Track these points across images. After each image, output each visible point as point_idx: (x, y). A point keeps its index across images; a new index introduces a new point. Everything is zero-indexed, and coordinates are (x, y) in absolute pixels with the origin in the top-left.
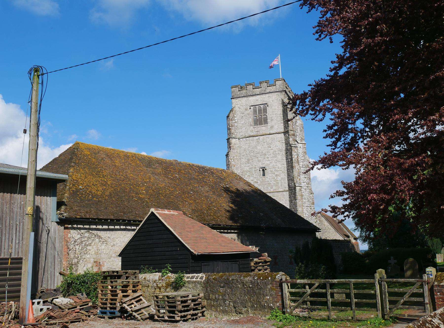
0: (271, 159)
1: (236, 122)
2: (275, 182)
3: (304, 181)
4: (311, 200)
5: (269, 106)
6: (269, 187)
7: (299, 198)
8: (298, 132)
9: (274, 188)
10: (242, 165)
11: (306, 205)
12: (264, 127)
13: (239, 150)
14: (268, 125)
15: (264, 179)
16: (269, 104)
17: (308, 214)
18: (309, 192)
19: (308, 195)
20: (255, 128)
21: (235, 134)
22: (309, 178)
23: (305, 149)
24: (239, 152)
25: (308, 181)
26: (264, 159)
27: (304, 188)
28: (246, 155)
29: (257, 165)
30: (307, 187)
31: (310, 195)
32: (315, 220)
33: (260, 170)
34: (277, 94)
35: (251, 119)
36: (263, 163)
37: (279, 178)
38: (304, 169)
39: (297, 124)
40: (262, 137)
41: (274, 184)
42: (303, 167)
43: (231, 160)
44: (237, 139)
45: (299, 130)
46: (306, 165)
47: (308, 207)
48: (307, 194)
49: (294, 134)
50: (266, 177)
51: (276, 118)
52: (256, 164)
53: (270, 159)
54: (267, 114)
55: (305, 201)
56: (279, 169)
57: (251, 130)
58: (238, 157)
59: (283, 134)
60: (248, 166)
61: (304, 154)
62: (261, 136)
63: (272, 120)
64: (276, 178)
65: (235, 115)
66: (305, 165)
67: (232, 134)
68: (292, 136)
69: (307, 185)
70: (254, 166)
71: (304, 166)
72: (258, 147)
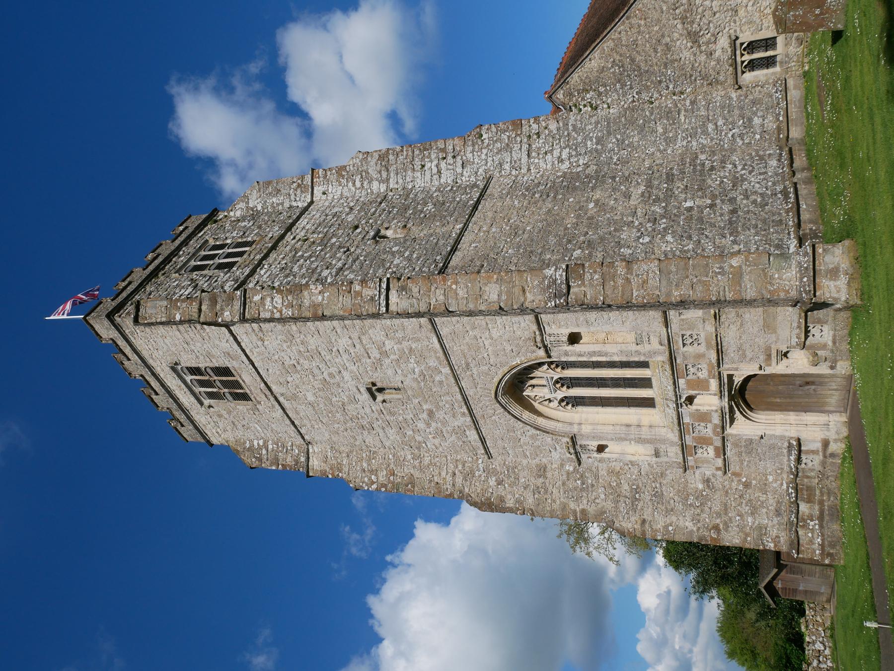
0: (333, 366)
1: (265, 442)
2: (412, 361)
3: (435, 170)
4: (504, 137)
5: (176, 359)
6: (437, 378)
7: (442, 297)
8: (282, 204)
9: (432, 363)
10: (387, 444)
12: (244, 378)
13: (342, 448)
14: (229, 366)
15: (410, 393)
16: (171, 359)
17: (562, 149)
18: (473, 145)
19: (485, 151)
20: (258, 399)
21: (297, 451)
22: (425, 149)
23: (329, 173)
24: (349, 447)
25: (433, 156)
26: (338, 385)
27: (459, 170)
28: (349, 431)
29: (368, 405)
30: (454, 157)
31: (487, 141)
32: (584, 110)
33: (384, 401)
34: (132, 339)
35: (238, 407)
36: (355, 390)
37: (389, 345)
38: (392, 175)
39: (259, 208)
40: (274, 388)
41: (417, 363)
42: (388, 180)
43: (373, 483)
44: (311, 450)
45: (274, 200)
46: (378, 168)
47: (534, 146)
48: (483, 157)
49: (210, 299)
50: (400, 385)
51: (199, 345)
52: (368, 410)
53: (332, 370)
54: (200, 366)
55: (507, 166)
56: (358, 346)
57: (269, 409)
58: (364, 455)
59: (232, 328)
60: (381, 431)
61: (343, 177)
62: (273, 390)
63: (209, 355)
64: (392, 357)
65: (248, 445)
66: (380, 172)
67: (297, 462)
68: (218, 307)
69: (450, 160)
70: (376, 415)
71: (384, 174)
72: (311, 398)
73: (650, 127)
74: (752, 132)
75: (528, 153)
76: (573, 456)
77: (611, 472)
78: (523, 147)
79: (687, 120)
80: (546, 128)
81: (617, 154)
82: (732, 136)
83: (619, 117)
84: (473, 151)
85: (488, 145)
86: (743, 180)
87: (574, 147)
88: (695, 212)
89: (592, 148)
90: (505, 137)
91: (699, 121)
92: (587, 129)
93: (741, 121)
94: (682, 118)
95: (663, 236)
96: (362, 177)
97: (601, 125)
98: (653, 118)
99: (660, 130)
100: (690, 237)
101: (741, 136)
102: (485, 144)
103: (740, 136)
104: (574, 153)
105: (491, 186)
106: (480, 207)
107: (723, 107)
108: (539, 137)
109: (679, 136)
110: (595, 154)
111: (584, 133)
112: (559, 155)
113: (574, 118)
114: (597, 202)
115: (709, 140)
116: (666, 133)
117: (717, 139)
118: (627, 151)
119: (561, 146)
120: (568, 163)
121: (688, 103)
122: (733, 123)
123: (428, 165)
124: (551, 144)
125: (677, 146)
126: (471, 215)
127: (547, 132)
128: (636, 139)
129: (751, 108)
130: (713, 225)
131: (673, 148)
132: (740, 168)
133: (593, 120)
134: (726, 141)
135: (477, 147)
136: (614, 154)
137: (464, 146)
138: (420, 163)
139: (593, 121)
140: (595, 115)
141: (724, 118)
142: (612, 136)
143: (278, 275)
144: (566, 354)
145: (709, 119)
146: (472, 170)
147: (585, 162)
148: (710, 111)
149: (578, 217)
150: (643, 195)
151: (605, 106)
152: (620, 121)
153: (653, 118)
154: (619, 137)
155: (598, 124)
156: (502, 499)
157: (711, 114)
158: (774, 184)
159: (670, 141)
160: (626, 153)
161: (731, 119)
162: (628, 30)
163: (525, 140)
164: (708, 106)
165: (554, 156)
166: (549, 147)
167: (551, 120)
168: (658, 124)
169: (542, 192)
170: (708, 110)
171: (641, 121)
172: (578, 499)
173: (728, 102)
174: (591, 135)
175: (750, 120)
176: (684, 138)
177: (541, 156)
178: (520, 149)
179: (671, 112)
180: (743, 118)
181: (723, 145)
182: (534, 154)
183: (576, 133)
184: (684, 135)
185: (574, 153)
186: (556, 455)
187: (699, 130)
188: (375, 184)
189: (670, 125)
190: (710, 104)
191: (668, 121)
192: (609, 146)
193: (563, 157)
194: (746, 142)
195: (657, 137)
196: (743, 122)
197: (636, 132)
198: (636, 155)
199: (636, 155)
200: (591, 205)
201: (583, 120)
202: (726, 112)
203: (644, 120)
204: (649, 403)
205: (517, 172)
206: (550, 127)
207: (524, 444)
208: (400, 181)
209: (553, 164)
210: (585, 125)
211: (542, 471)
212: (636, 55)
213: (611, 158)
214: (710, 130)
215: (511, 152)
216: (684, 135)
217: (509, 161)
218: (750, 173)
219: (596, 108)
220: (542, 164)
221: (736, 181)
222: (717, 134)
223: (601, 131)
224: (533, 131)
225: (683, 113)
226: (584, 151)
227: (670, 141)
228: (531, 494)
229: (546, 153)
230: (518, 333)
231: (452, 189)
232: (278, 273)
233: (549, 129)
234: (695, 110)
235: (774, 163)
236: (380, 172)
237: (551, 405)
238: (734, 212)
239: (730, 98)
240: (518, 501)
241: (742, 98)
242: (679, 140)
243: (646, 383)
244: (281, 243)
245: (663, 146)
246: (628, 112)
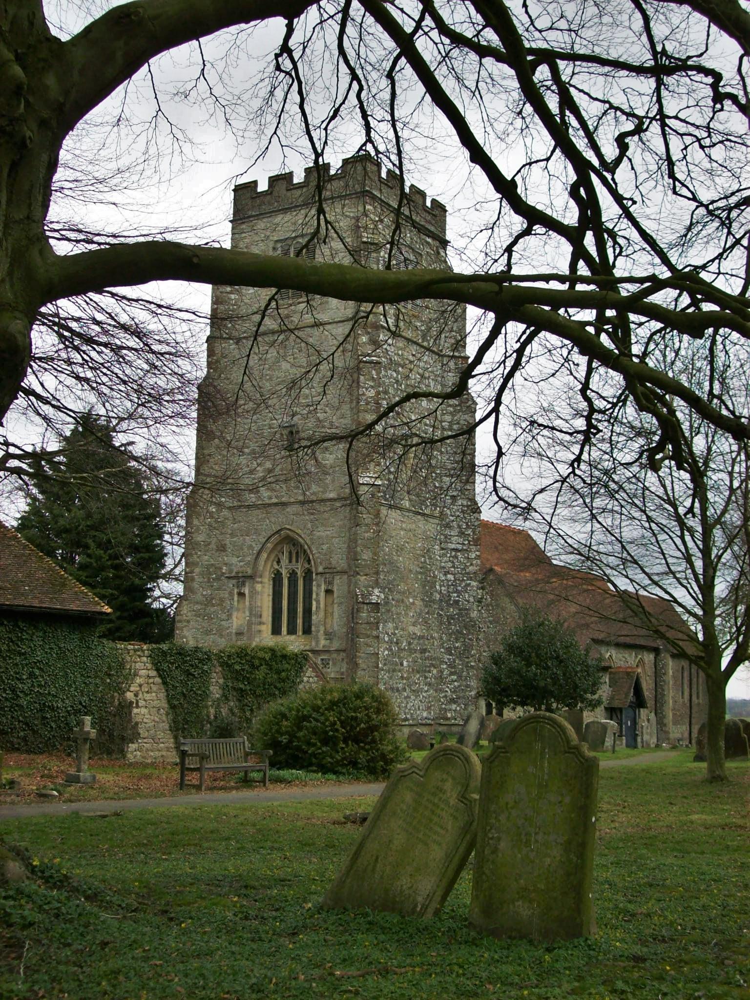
4: (469, 532)
11: (453, 546)
66: (458, 423)
76: (233, 574)
77: (222, 600)
84: (462, 505)
85: (465, 518)
86: (416, 697)
88: (399, 667)
95: (387, 649)
96: (456, 406)
100: (385, 664)
101: (446, 696)
110: (447, 599)
114: (413, 603)
122: (455, 692)
130: (391, 678)
132: (424, 694)
133: (472, 599)
141: (459, 686)
144: (319, 586)
149: (404, 593)
150: (414, 634)
156: (198, 515)
158: (412, 714)
169: (425, 562)
172: (201, 574)
175: (455, 703)
182: (453, 553)
186: (234, 560)
188: (448, 418)
193: (449, 576)
200: (411, 600)
204: (276, 631)
207: (244, 539)
211: (222, 548)
218: (421, 701)
221: (416, 692)
228: (203, 539)
229: (453, 562)
230: (336, 557)
235: (425, 714)
237: (275, 563)
238: (398, 690)
239: (470, 691)
240: (198, 529)
243: (292, 631)
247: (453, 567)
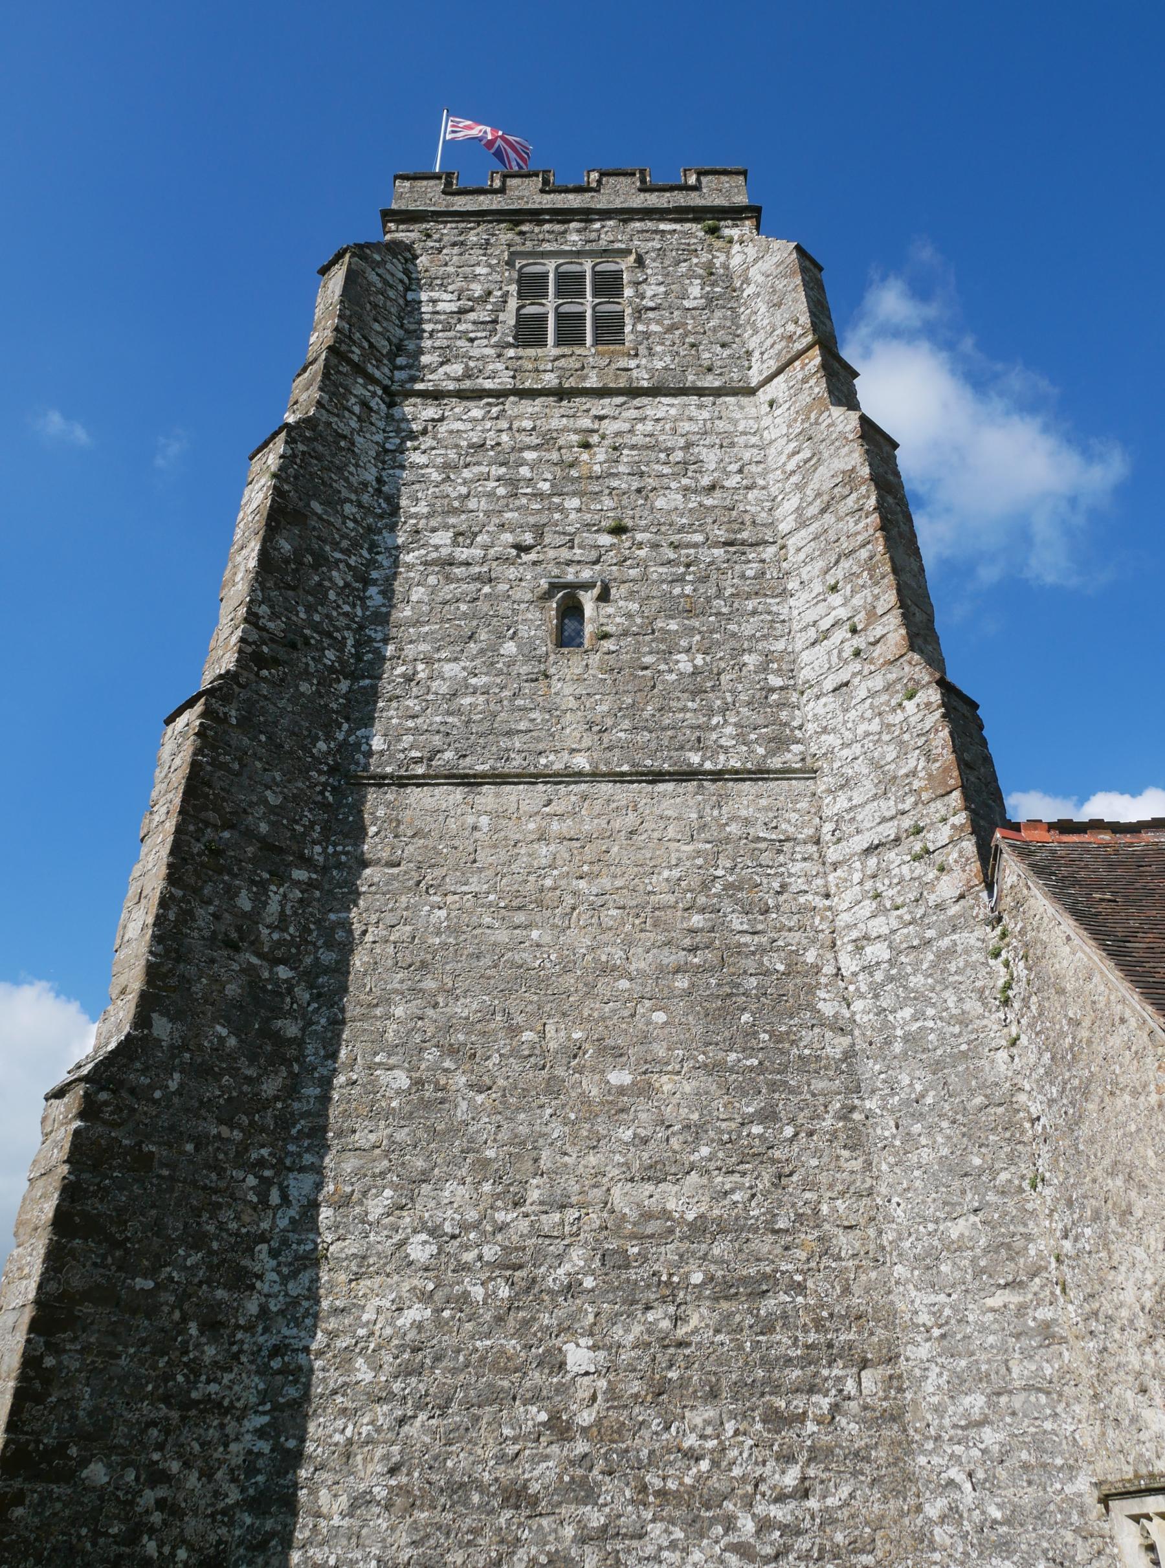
3: (825, 624)
4: (914, 760)
18: (887, 688)
22: (871, 570)
27: (829, 685)
30: (857, 653)
31: (899, 716)
32: (997, 964)
47: (892, 855)
48: (862, 728)
71: (813, 510)
73: (964, 1192)
74: (966, 1554)
75: (877, 847)
78: (891, 824)
79: (990, 1316)
80: (942, 869)
81: (883, 1108)
82: (951, 1483)
83: (983, 1086)
87: (894, 972)
89: (895, 1028)
90: (912, 763)
91: (989, 1362)
92: (946, 994)
93: (997, 1514)
94: (996, 1301)
97: (960, 1034)
98: (991, 1197)
99: (956, 1230)
101: (952, 1514)
102: (891, 719)
103: (951, 1509)
104: (879, 976)
105: (772, 784)
106: (661, 787)
107: (1038, 1444)
108: (917, 858)
109: (942, 1298)
110: (878, 1040)
111: (933, 990)
112: (874, 935)
113: (972, 941)
115: (935, 1400)
116: (948, 1250)
117: (941, 1427)
118: (894, 1137)
119: (893, 932)
120: (854, 969)
121: (1045, 1313)
123: (836, 599)
124: (899, 901)
125: (913, 1293)
126: (619, 778)
127: (932, 875)
128: (926, 1155)
129: (1045, 1552)
131: (908, 1281)
133: (973, 1006)
134: (935, 1460)
135: (884, 697)
136: (883, 1098)
137: (883, 665)
138: (841, 577)
139: (967, 1006)
140: (985, 1005)
142: (930, 1077)
143: (457, 446)
145: (999, 1394)
146: (830, 715)
147: (857, 1017)
148: (1024, 1394)
151: (1014, 1030)
152: (972, 1092)
153: (991, 1197)
154: (929, 1100)
155: (961, 1023)
157: (1017, 1401)
159: (928, 1268)
160: (887, 1134)
161: (1002, 1474)
162: (1134, 1049)
163: (907, 823)
164: (1039, 1390)
165: (871, 923)
166: (892, 898)
167: (965, 876)
168: (973, 1218)
170: (1027, 1388)
171: (977, 1161)
173: (1059, 1461)
174: (930, 1012)
176: (937, 1315)
177: (868, 885)
178: (884, 820)
179: (1011, 1259)
180: (1007, 1522)
181: (923, 1452)
182: (872, 862)
183: (934, 966)
184: (947, 1312)
185: (879, 976)
187: (963, 1363)
189: (974, 1261)
190: (1048, 1393)
191: (986, 1251)
192: (904, 1075)
194: (937, 1530)
195: (936, 1222)
196: (995, 1521)
197: (945, 1151)
198: (884, 1167)
199: (884, 1167)
200: (620, 1077)
201: (969, 971)
202: (1024, 1455)
203: (981, 1171)
205: (828, 837)
206: (945, 878)
208: (802, 555)
209: (848, 927)
210: (956, 986)
212: (1097, 1100)
213: (873, 1092)
214: (967, 1401)
215: (875, 797)
216: (947, 1312)
217: (854, 802)
219: (1006, 1002)
220: (849, 896)
222: (955, 1426)
223: (942, 1038)
224: (930, 836)
225: (1012, 1298)
226: (885, 1005)
227: (928, 1268)
231: (772, 690)
232: (464, 443)
233: (937, 878)
234: (1025, 1342)
236: (819, 495)
239: (1071, 1470)
241: (1075, 1517)
242: (933, 1298)
244: (584, 400)
245: (913, 1246)
246: (1001, 1110)
247: (881, 911)
